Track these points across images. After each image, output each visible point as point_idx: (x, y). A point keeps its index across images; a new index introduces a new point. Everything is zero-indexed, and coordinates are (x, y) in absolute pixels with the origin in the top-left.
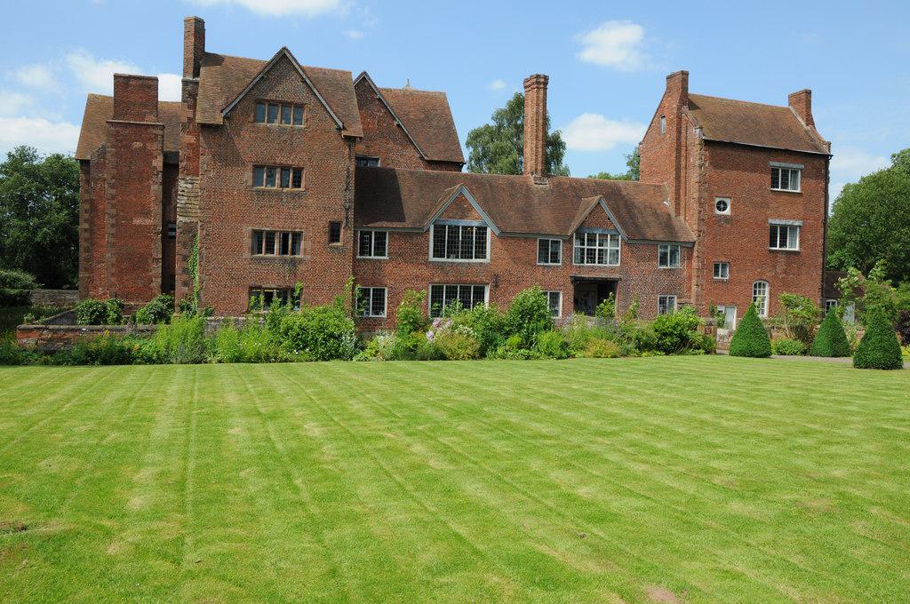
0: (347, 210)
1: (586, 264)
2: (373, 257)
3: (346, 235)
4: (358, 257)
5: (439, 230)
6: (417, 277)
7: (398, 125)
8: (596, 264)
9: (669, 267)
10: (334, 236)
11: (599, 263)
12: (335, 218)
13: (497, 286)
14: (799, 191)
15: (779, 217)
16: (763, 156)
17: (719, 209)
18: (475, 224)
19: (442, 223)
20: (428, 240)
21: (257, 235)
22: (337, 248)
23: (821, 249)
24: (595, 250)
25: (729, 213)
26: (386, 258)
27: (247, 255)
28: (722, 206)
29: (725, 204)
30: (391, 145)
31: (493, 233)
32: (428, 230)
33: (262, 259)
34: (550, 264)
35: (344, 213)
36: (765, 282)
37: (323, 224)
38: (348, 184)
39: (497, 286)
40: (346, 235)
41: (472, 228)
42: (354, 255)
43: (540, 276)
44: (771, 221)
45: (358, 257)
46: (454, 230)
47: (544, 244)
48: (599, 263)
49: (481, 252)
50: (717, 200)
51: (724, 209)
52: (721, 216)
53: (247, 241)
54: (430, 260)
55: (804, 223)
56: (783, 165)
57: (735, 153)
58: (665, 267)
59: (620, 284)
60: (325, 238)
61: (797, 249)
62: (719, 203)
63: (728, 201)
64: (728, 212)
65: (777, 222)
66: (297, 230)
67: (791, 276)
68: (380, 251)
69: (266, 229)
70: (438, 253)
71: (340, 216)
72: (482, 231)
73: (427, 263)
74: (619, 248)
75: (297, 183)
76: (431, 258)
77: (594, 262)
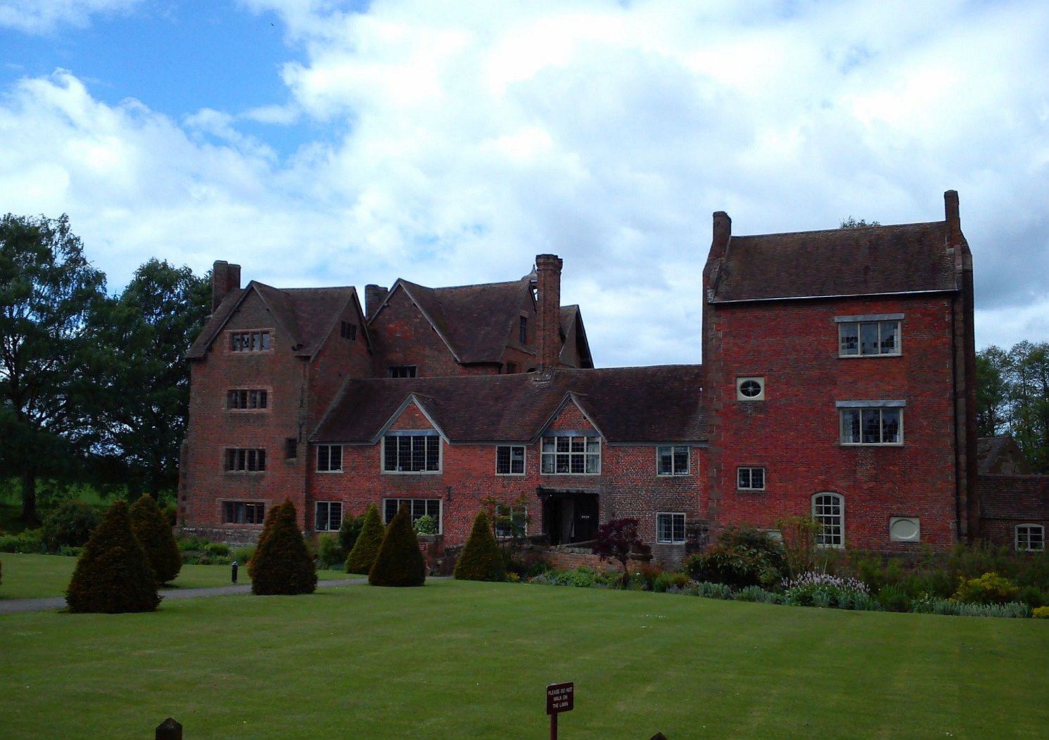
0: (301, 427)
1: (556, 474)
2: (330, 471)
3: (302, 449)
4: (317, 472)
5: (390, 441)
6: (369, 491)
7: (433, 329)
8: (570, 474)
9: (673, 475)
10: (291, 447)
11: (572, 472)
12: (291, 435)
13: (449, 500)
14: (899, 354)
15: (857, 396)
16: (821, 310)
17: (746, 393)
18: (430, 434)
19: (393, 434)
20: (379, 453)
21: (231, 453)
22: (292, 464)
23: (949, 441)
24: (568, 456)
25: (763, 399)
26: (341, 472)
27: (222, 472)
28: (751, 389)
29: (757, 386)
30: (427, 351)
31: (445, 443)
32: (379, 442)
33: (233, 475)
34: (511, 474)
35: (298, 429)
36: (837, 495)
37: (281, 440)
38: (302, 402)
39: (449, 500)
40: (302, 449)
41: (396, 437)
42: (310, 468)
43: (499, 488)
44: (839, 404)
45: (317, 472)
46: (404, 440)
47: (504, 454)
48: (572, 472)
49: (433, 465)
50: (741, 381)
51: (754, 394)
52: (745, 403)
53: (222, 460)
54: (382, 473)
55: (909, 403)
56: (860, 318)
57: (767, 313)
58: (667, 475)
59: (290, 500)
60: (282, 455)
61: (899, 441)
62: (745, 385)
63: (761, 382)
64: (760, 397)
65: (853, 404)
66: (261, 448)
67: (887, 486)
68: (336, 465)
69: (238, 448)
70: (390, 465)
71: (294, 434)
72: (434, 440)
73: (378, 476)
74: (600, 453)
75: (263, 405)
76: (383, 471)
77: (582, 471)
